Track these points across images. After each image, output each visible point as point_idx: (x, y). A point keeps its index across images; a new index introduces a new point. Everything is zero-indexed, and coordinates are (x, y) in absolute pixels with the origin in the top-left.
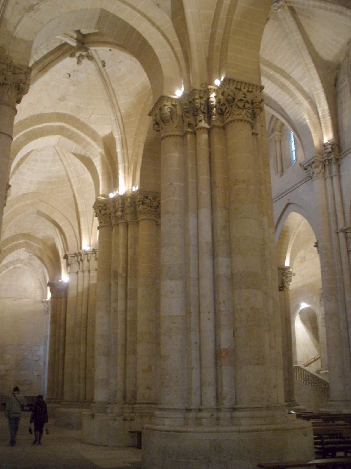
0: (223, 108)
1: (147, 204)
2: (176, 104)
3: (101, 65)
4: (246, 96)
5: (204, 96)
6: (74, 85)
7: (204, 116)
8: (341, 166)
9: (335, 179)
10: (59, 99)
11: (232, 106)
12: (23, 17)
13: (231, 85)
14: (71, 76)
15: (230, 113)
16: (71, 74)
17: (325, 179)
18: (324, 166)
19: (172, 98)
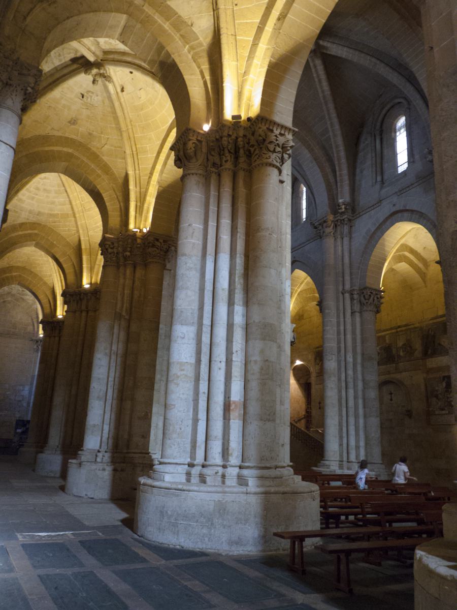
0: (252, 149)
1: (157, 246)
2: (202, 140)
3: (119, 90)
4: (278, 139)
5: (233, 134)
6: (87, 109)
7: (231, 156)
8: (353, 228)
9: (346, 240)
10: (69, 122)
11: (261, 148)
12: (35, 6)
13: (263, 124)
14: (85, 97)
15: (259, 156)
16: (85, 94)
17: (335, 240)
18: (336, 226)
19: (199, 133)
